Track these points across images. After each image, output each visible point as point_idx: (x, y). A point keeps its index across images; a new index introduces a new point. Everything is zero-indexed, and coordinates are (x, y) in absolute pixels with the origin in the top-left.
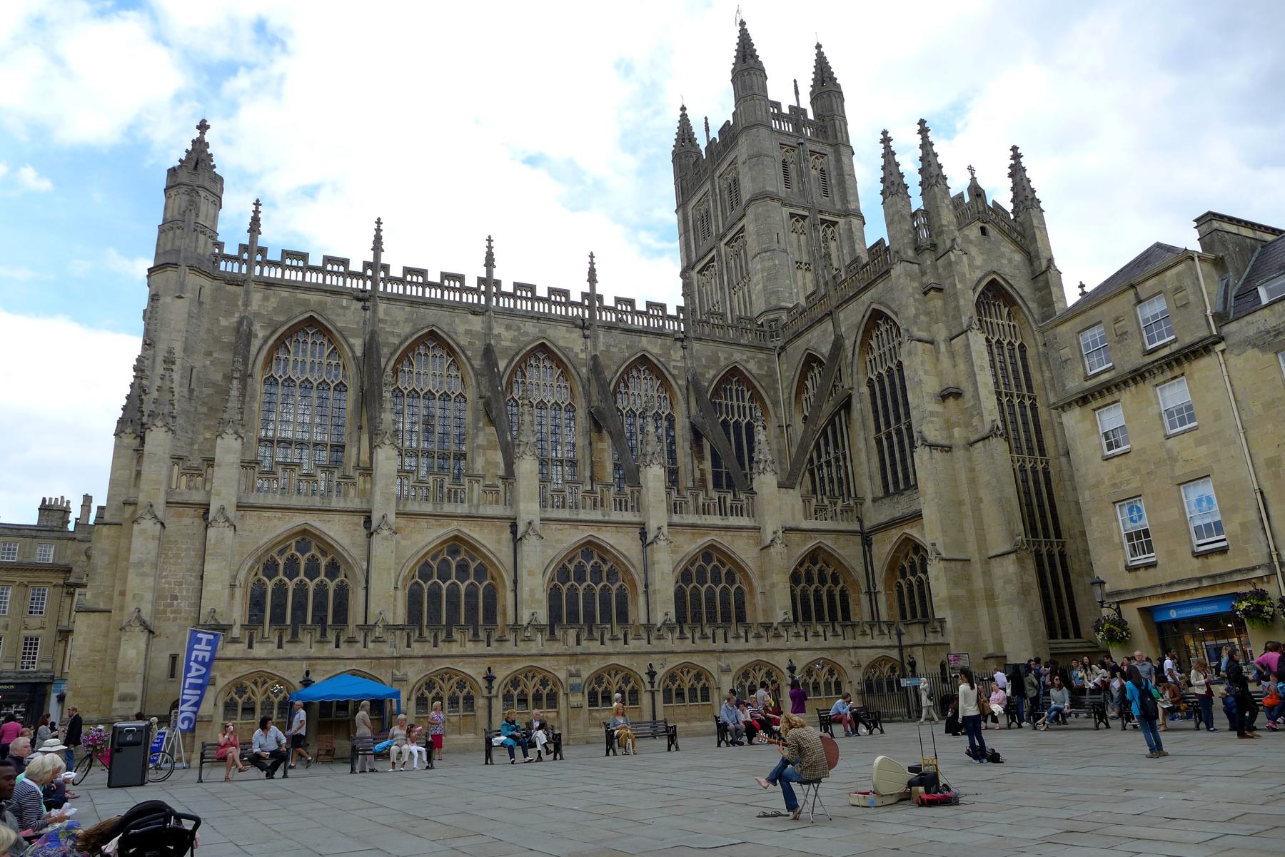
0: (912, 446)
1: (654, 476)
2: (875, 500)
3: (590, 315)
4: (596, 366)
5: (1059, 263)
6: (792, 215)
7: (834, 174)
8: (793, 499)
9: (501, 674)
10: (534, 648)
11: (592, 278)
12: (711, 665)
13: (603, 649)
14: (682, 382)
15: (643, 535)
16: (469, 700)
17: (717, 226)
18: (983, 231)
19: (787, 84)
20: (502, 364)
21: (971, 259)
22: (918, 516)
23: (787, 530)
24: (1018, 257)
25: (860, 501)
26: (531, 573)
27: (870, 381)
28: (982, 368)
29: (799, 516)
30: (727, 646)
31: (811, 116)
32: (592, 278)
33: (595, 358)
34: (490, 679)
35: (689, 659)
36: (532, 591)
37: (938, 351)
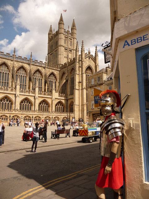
0: (73, 89)
1: (37, 89)
4: (30, 71)
6: (65, 49)
7: (73, 43)
8: (57, 94)
10: (16, 113)
11: (31, 57)
12: (41, 116)
13: (26, 113)
14: (44, 74)
15: (35, 98)
16: (7, 119)
17: (54, 48)
20: (15, 69)
27: (71, 78)
29: (58, 96)
30: (44, 114)
31: (70, 32)
32: (31, 57)
35: (38, 115)
36: (17, 105)
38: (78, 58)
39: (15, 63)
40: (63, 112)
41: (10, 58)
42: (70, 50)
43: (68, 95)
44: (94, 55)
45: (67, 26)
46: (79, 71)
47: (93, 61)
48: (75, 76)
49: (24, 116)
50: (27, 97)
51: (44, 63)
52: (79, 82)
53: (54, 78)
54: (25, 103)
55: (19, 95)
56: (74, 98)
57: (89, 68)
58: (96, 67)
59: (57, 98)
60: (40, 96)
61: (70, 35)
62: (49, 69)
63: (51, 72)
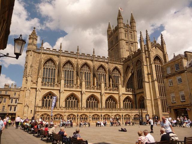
1: (103, 85)
2: (137, 89)
3: (93, 58)
4: (94, 67)
5: (167, 53)
6: (126, 42)
7: (133, 35)
9: (80, 114)
11: (94, 53)
13: (94, 111)
14: (107, 69)
15: (101, 95)
16: (75, 118)
17: (114, 43)
18: (156, 48)
19: (126, 20)
20: (79, 66)
21: (153, 52)
22: (143, 92)
23: (123, 94)
24: (161, 52)
25: (135, 89)
26: (84, 99)
28: (154, 70)
29: (125, 91)
30: (113, 112)
31: (130, 26)
32: (94, 53)
33: (94, 65)
34: (78, 116)
36: (84, 102)
37: (147, 67)
38: (143, 49)
39: (79, 60)
40: (132, 108)
41: (74, 56)
42: (131, 43)
43: (136, 90)
44: (160, 43)
45: (126, 20)
46: (147, 62)
47: (160, 50)
48: (143, 67)
49: (92, 114)
50: (93, 93)
51: (106, 58)
52: (148, 74)
53: (118, 73)
54: (91, 100)
55: (85, 92)
56: (144, 92)
57: (157, 58)
58: (165, 56)
59: (124, 93)
60: (106, 92)
61: (129, 29)
62: (112, 64)
63: (114, 66)
